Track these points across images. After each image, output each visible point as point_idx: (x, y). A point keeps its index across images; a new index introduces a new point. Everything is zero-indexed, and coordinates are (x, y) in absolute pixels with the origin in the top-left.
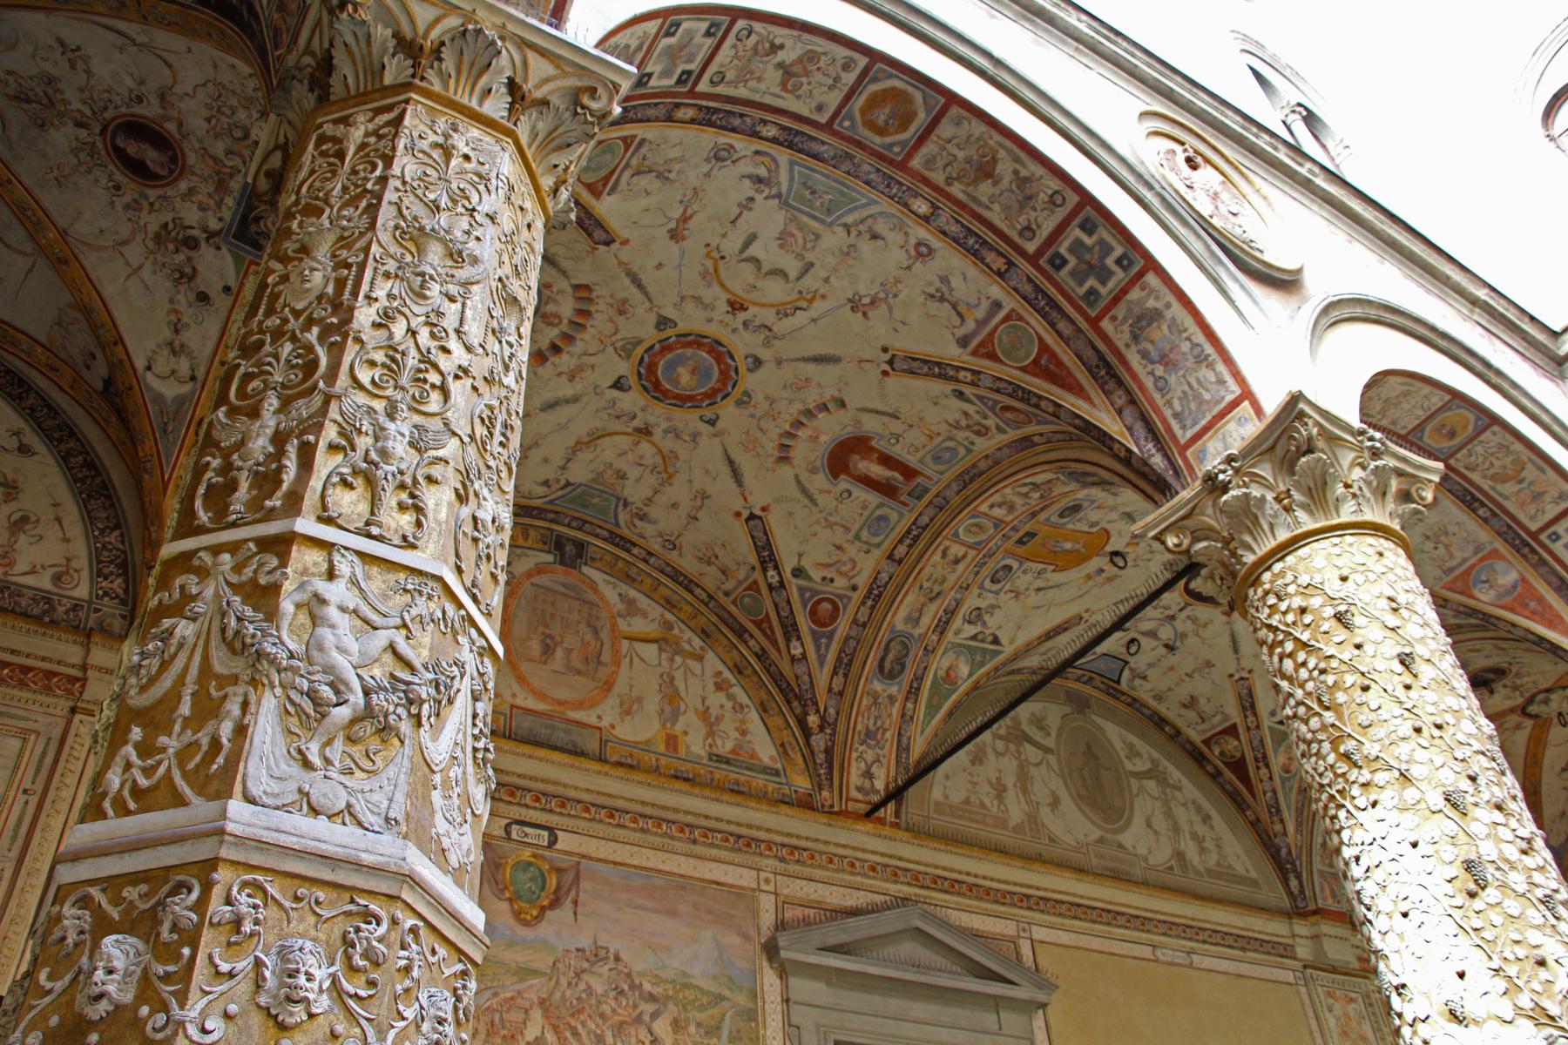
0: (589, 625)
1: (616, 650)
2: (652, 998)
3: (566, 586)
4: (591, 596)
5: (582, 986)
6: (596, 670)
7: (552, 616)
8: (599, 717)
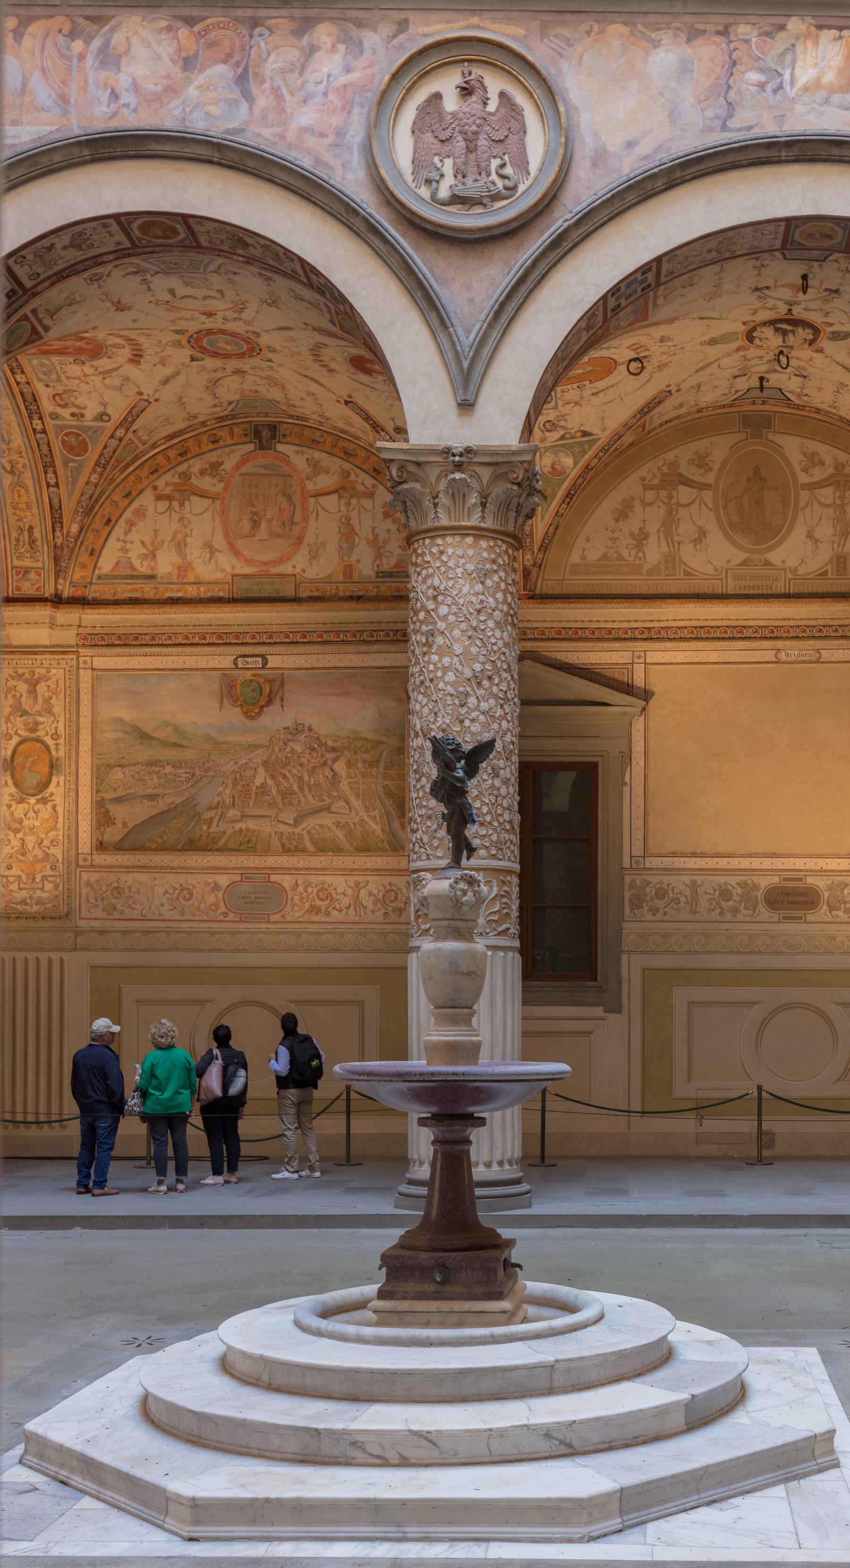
3: (265, 467)
4: (285, 469)
6: (291, 530)
7: (257, 495)
8: (294, 567)
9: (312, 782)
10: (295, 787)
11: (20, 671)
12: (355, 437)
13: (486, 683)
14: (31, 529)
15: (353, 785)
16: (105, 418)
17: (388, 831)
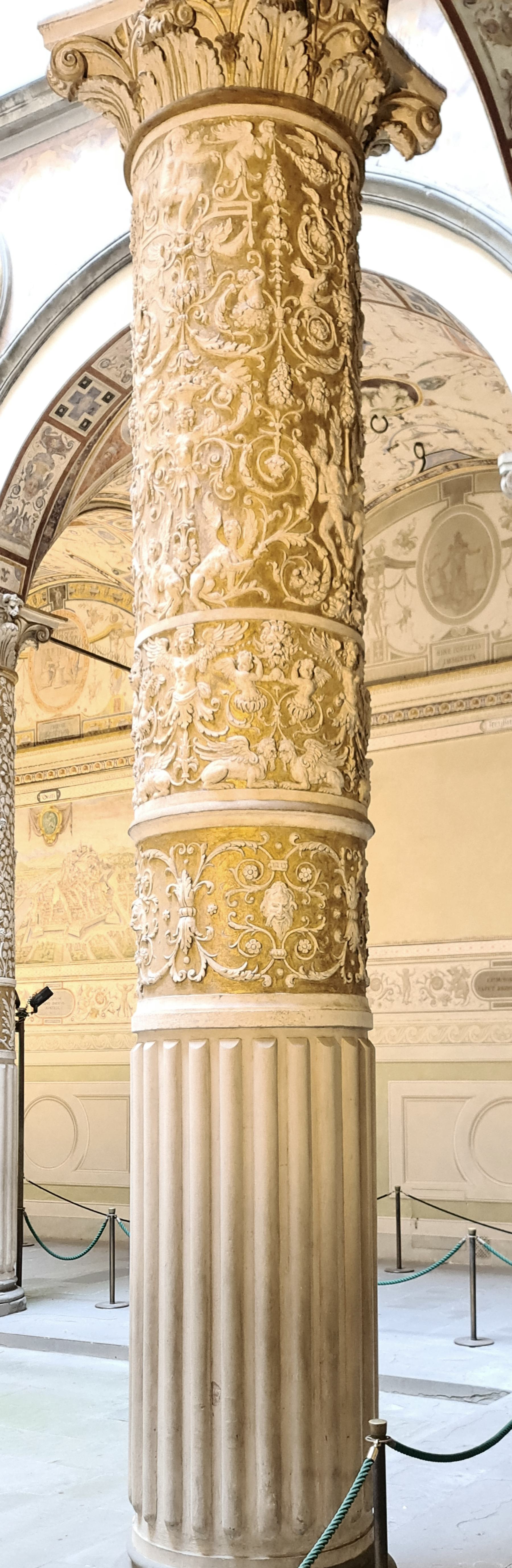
5: (76, 870)
8: (79, 707)
10: (81, 904)
15: (124, 897)
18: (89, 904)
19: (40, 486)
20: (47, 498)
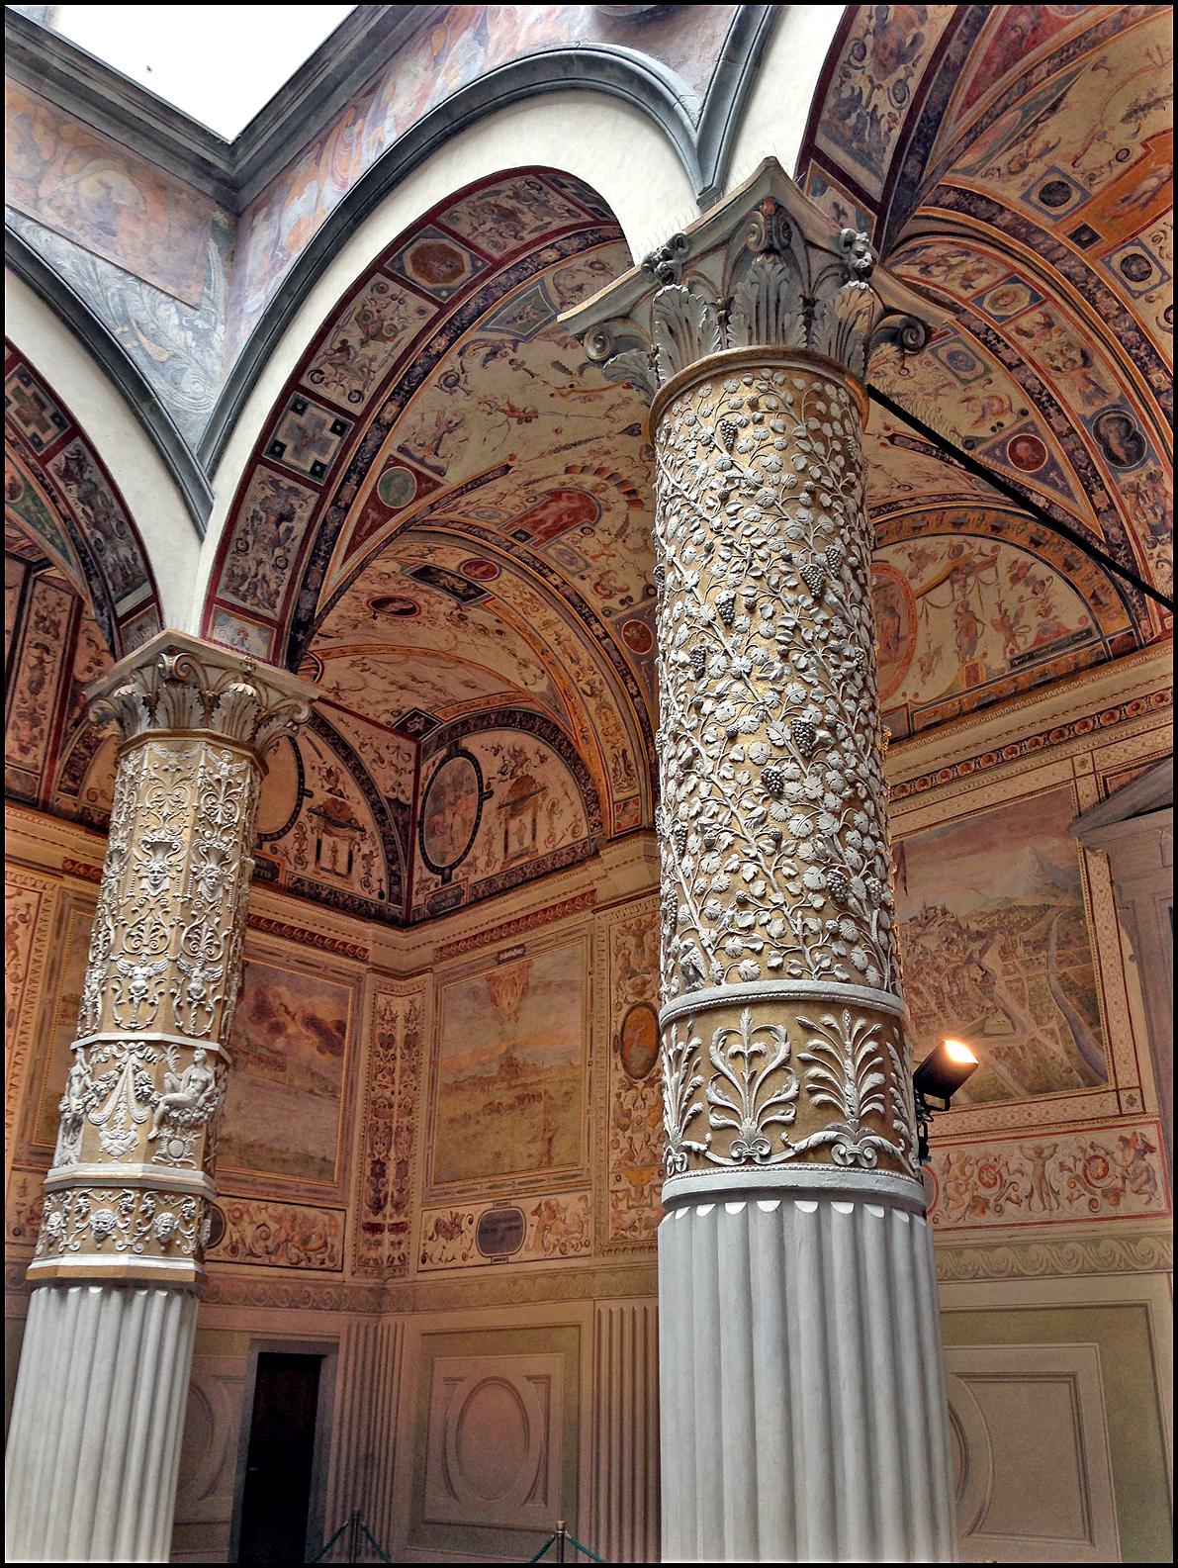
0: (886, 608)
1: (912, 617)
2: (980, 935)
5: (919, 949)
6: (897, 650)
9: (955, 993)
11: (628, 924)
12: (957, 497)
13: (741, 620)
14: (625, 752)
15: (1015, 985)
16: (651, 591)
17: (1075, 1051)
18: (948, 1004)
19: (901, 56)
20: (913, 84)
